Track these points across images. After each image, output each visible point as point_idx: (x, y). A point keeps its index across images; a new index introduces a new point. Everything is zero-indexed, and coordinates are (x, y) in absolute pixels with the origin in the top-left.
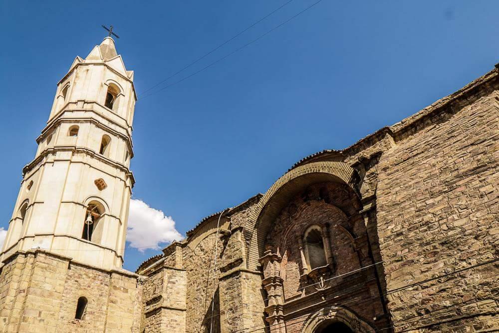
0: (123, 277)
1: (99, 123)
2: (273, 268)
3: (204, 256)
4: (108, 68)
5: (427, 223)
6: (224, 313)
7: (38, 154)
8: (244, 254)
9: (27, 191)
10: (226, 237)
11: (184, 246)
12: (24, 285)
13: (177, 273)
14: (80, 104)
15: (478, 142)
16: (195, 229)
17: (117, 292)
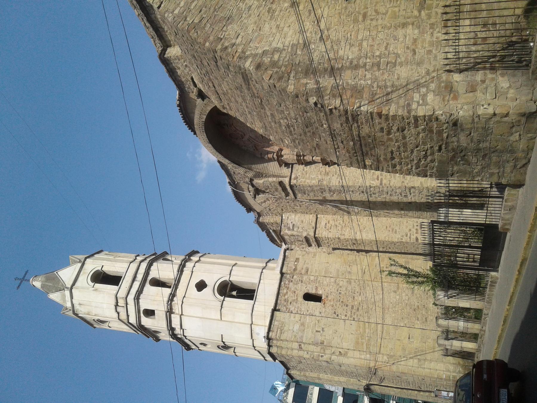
0: (285, 263)
1: (137, 291)
2: (288, 156)
3: (271, 201)
4: (74, 284)
5: (288, 125)
6: (324, 197)
7: (175, 341)
8: (275, 179)
9: (208, 346)
10: (257, 191)
11: (259, 215)
12: (296, 345)
13: (285, 222)
14: (119, 309)
15: (215, 60)
16: (245, 207)
17: (299, 268)
